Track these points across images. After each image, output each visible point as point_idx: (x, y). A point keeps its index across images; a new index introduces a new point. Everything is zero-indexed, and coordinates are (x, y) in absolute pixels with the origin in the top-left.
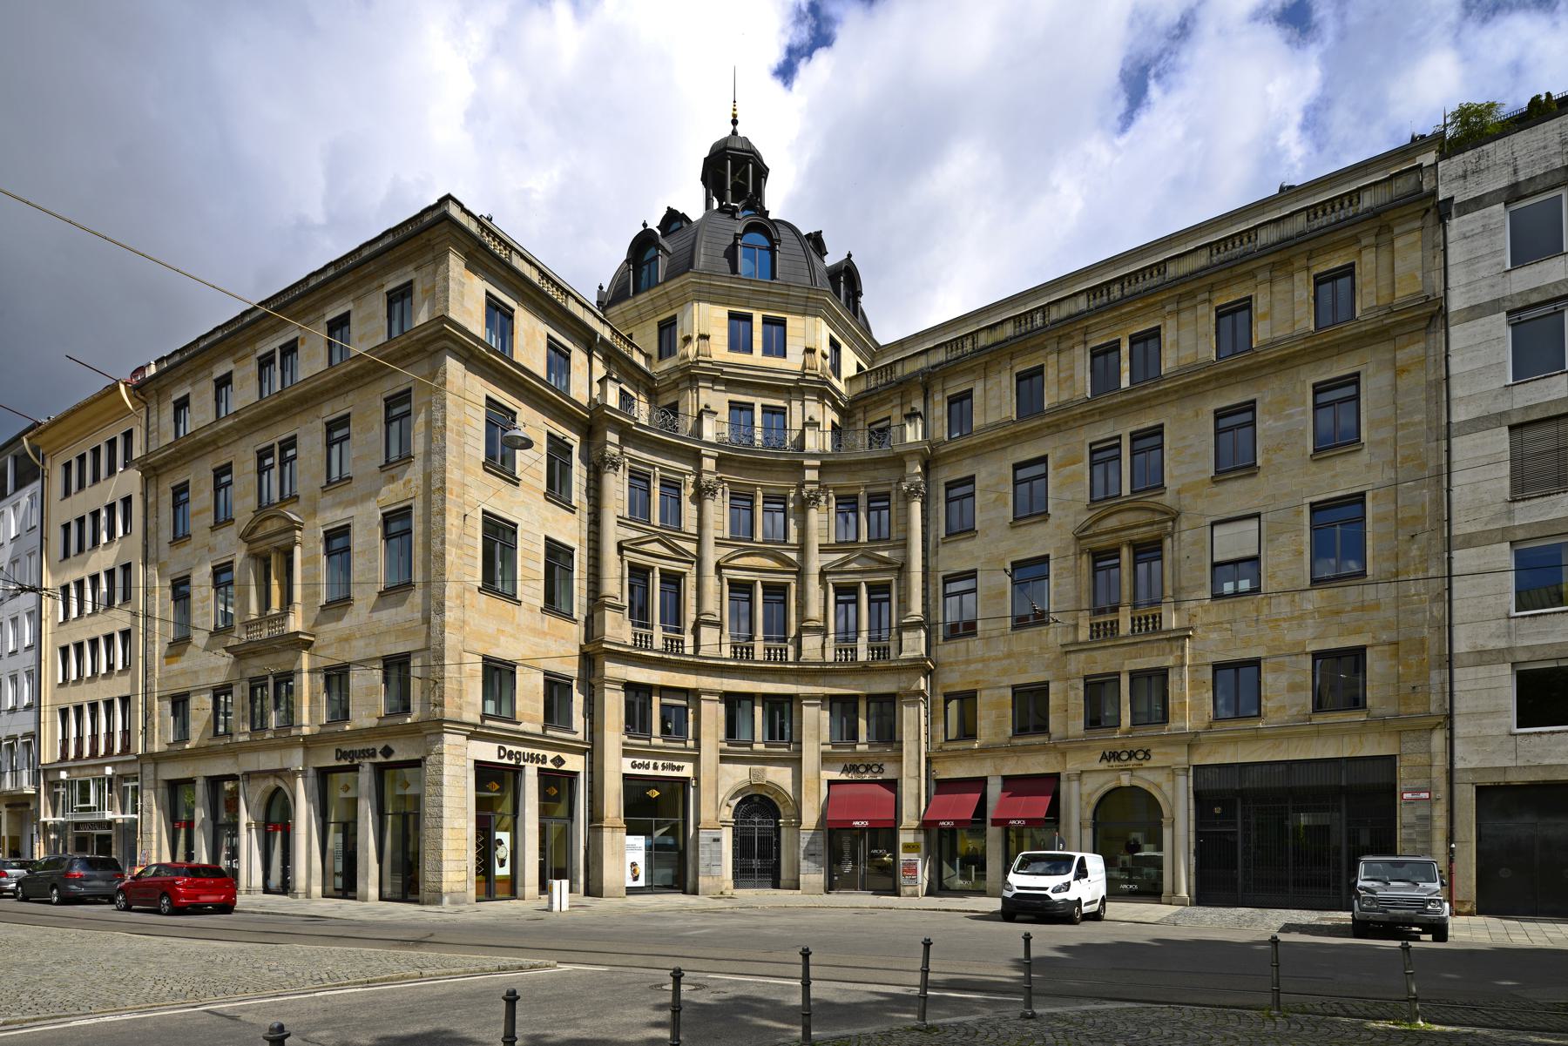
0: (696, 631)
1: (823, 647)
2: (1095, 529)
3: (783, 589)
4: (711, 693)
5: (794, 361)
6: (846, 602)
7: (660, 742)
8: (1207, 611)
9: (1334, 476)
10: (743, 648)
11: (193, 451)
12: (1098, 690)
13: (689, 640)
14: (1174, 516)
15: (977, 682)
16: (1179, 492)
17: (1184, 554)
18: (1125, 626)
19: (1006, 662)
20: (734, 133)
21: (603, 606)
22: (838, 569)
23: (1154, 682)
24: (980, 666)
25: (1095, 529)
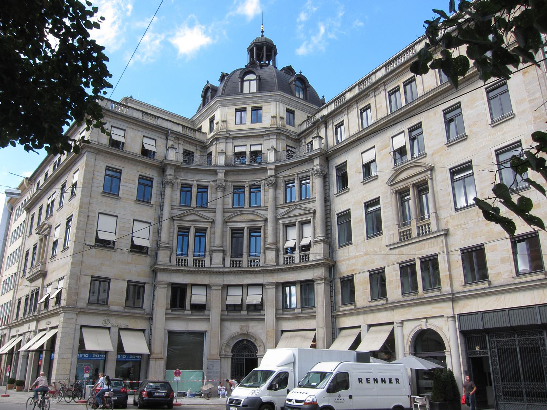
0: (211, 255)
1: (224, 259)
2: (397, 180)
3: (204, 230)
4: (216, 285)
5: (266, 122)
6: (183, 236)
7: (189, 312)
8: (453, 219)
9: (503, 134)
10: (182, 262)
11: (40, 197)
12: (407, 270)
13: (207, 260)
14: (432, 169)
15: (353, 270)
16: (432, 155)
17: (439, 188)
18: (414, 233)
19: (365, 257)
20: (262, 36)
21: (323, 241)
22: (180, 217)
23: (430, 263)
24: (354, 261)
25: (397, 180)
